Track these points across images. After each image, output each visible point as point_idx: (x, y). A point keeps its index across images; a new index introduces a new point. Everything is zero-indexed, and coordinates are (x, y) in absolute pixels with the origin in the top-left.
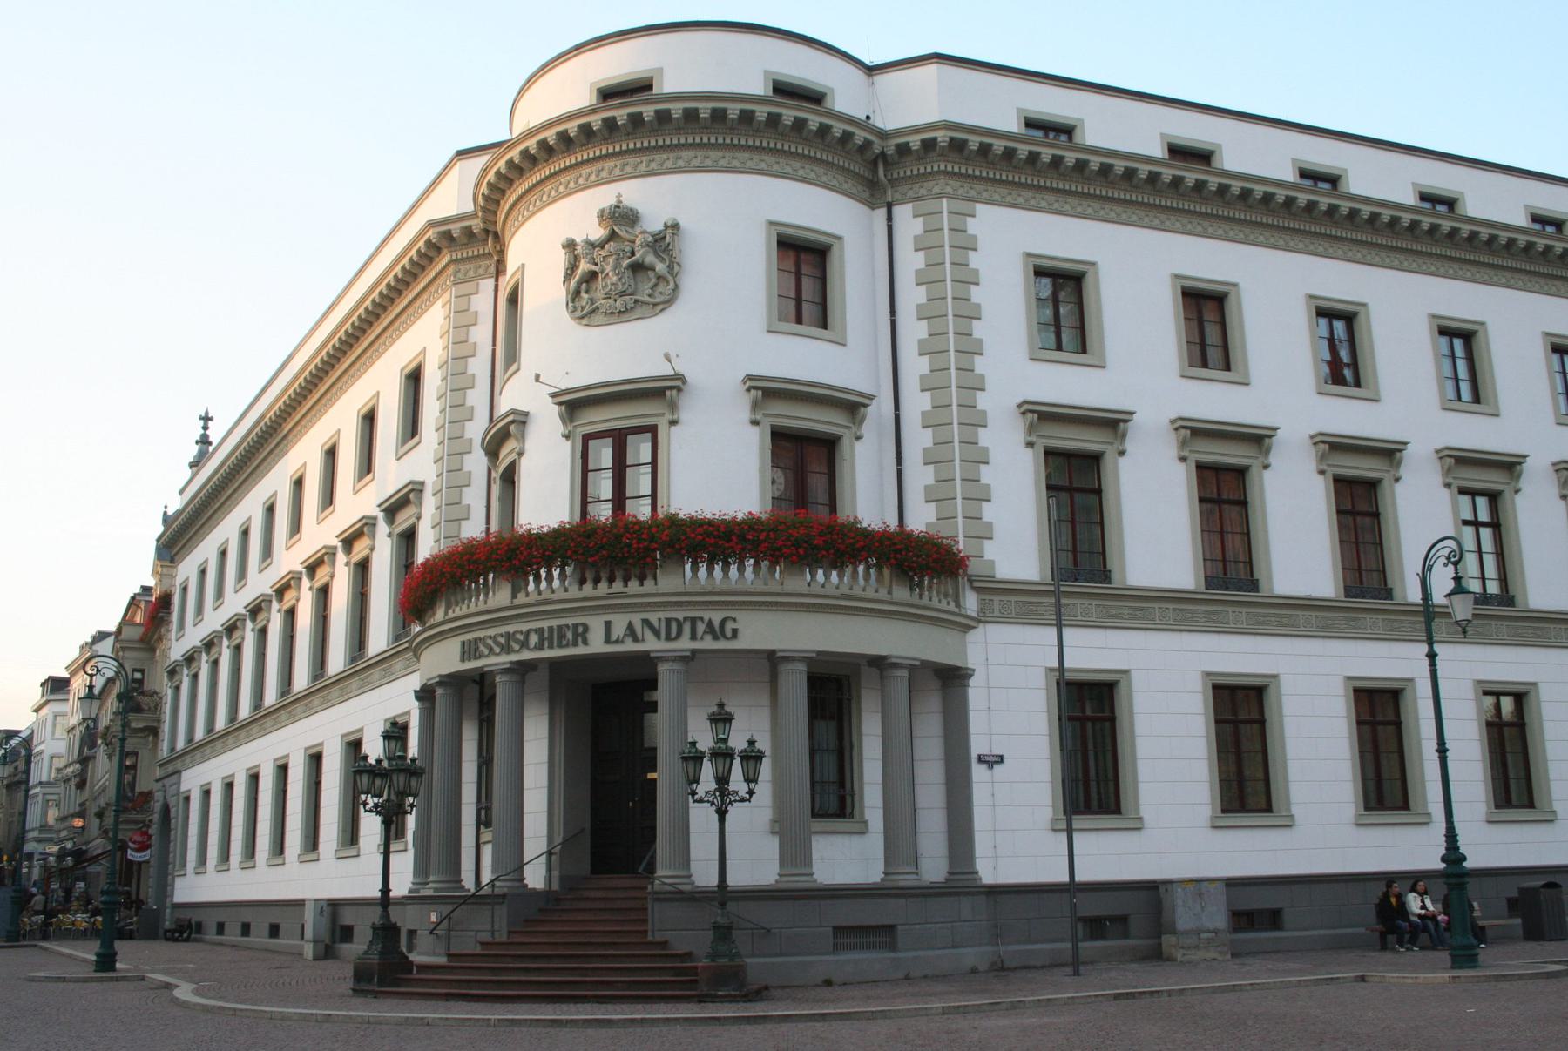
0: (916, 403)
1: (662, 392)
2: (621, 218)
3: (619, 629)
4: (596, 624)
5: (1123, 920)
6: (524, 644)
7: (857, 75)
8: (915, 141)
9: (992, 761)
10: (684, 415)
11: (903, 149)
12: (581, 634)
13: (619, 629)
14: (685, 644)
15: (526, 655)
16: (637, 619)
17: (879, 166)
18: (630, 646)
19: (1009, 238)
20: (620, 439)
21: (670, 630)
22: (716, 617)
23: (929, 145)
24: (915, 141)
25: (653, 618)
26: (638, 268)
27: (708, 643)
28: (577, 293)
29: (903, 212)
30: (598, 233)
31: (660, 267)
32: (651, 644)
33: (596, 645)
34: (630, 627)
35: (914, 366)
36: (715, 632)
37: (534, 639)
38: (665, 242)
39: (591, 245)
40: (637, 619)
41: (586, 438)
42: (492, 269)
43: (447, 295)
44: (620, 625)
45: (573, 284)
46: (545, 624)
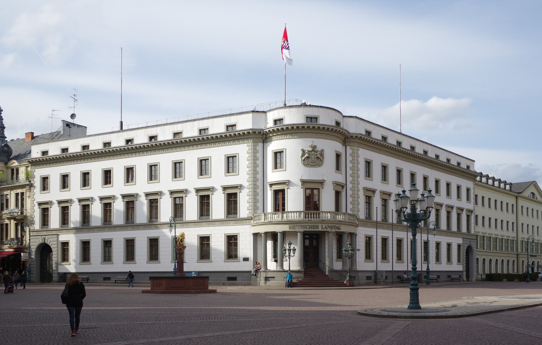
0: (349, 186)
1: (322, 183)
2: (314, 147)
3: (324, 227)
4: (320, 226)
5: (371, 277)
6: (306, 228)
7: (342, 117)
8: (354, 136)
9: (359, 250)
10: (324, 187)
11: (352, 137)
12: (318, 227)
13: (324, 227)
14: (334, 230)
15: (306, 230)
16: (327, 225)
17: (347, 139)
18: (326, 230)
19: (364, 154)
20: (312, 189)
21: (331, 228)
22: (338, 226)
23: (356, 137)
24: (354, 136)
25: (329, 225)
26: (318, 158)
27: (337, 230)
28: (304, 160)
29: (348, 148)
30: (310, 149)
31: (321, 158)
32: (329, 230)
33: (320, 229)
34: (326, 227)
35: (349, 179)
36: (338, 228)
37: (308, 227)
38: (322, 153)
39: (309, 151)
40: (327, 225)
41: (306, 189)
42: (262, 141)
43: (250, 144)
44: (324, 226)
45: (303, 158)
46: (310, 225)
